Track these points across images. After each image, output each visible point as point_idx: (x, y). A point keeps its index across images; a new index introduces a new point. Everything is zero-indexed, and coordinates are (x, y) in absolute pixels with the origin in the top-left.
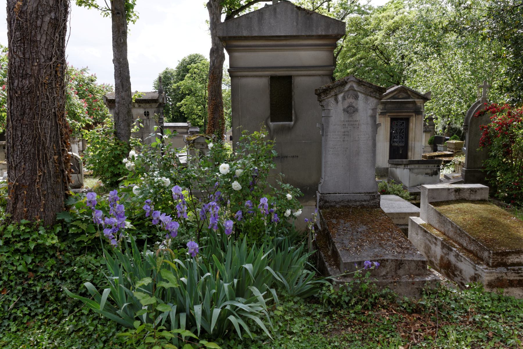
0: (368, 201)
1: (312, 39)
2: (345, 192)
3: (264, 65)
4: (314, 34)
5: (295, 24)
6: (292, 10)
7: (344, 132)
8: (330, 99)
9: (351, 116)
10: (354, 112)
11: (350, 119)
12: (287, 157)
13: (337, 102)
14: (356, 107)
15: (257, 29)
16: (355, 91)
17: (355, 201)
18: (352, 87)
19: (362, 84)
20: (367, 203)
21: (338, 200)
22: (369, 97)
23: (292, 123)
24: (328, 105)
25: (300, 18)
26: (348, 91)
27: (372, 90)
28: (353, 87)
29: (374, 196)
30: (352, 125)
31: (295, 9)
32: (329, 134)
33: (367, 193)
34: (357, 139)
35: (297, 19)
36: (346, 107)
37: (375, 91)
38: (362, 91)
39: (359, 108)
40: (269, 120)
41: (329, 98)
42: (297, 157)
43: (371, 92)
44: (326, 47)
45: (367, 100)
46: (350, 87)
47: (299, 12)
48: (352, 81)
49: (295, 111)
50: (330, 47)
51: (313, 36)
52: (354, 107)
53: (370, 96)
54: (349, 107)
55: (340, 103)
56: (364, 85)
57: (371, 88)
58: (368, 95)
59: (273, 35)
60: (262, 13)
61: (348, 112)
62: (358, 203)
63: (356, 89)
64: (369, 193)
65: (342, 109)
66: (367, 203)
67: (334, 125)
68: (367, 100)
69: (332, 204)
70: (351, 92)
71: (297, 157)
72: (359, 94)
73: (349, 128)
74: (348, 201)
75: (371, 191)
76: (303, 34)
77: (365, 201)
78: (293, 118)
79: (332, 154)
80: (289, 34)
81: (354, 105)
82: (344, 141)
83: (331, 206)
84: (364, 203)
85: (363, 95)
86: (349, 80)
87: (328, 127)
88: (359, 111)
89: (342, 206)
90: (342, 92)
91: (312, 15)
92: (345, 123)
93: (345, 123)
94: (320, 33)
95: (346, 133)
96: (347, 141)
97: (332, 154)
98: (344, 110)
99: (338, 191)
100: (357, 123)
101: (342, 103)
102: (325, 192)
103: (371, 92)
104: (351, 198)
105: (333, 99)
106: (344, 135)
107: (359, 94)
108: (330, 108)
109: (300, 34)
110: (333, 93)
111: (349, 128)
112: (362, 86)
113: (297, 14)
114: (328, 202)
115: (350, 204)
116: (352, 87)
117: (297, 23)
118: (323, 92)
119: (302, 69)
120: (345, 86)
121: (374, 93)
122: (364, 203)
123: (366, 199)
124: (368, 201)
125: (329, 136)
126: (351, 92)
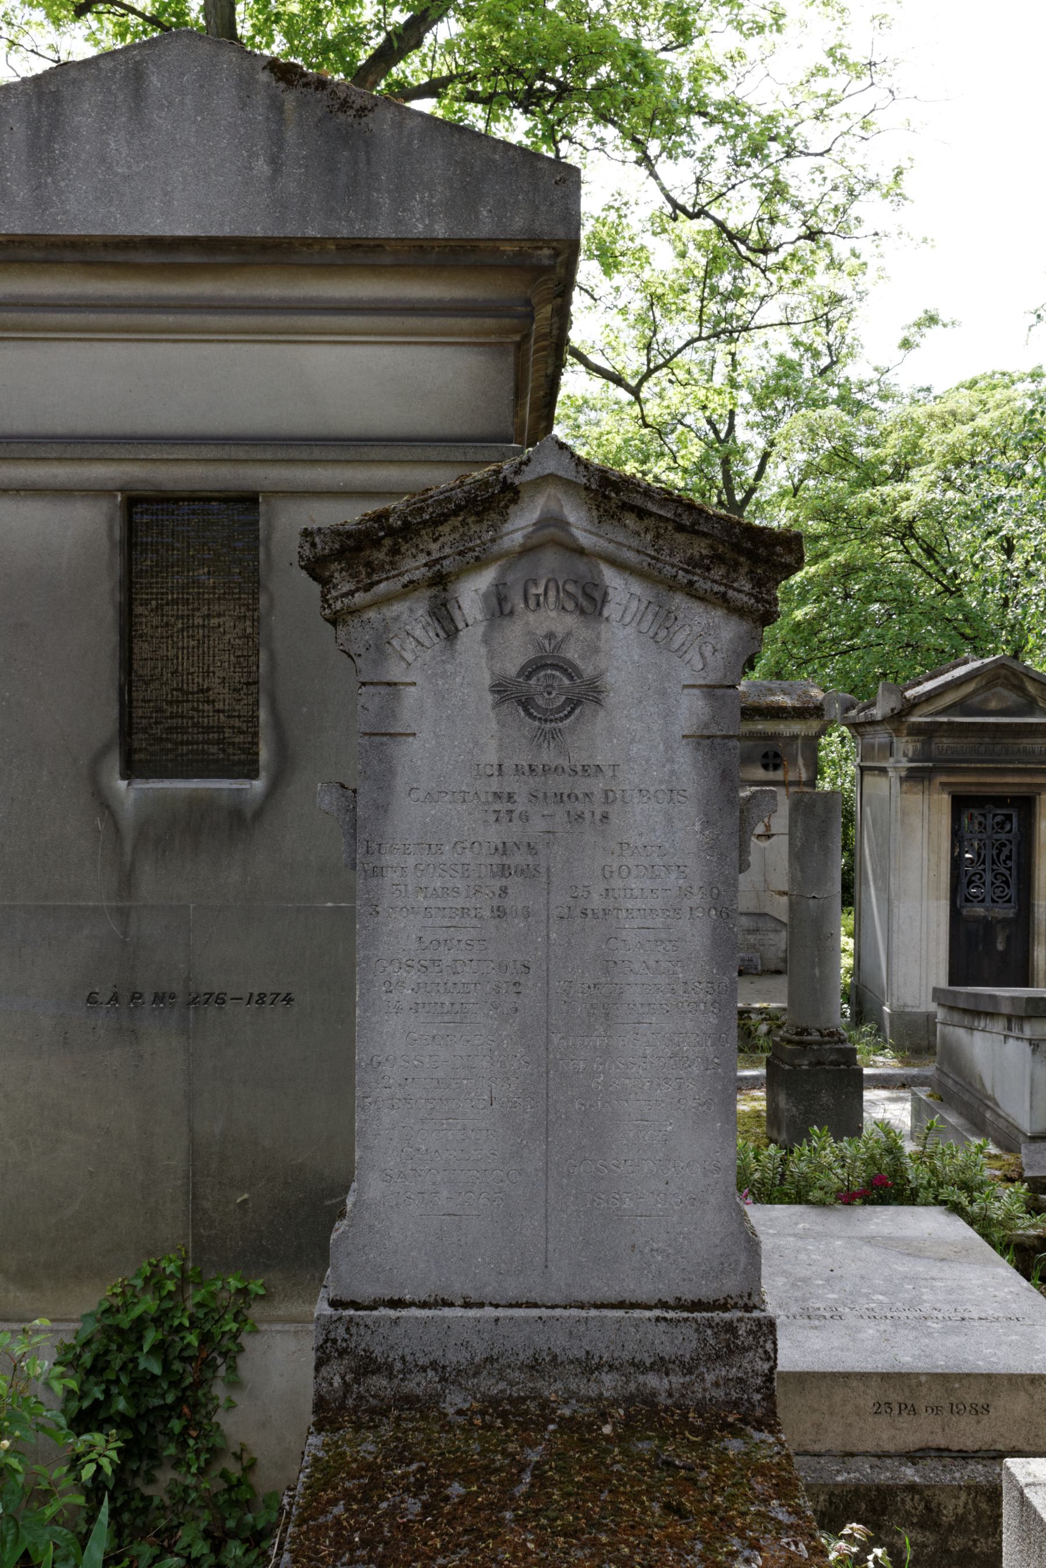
0: (688, 1369)
1: (375, 269)
2: (513, 1290)
3: (82, 425)
4: (383, 230)
5: (262, 167)
6: (245, 84)
7: (504, 849)
8: (397, 608)
9: (554, 734)
10: (573, 703)
11: (548, 756)
12: (220, 999)
13: (451, 634)
14: (588, 669)
15: (21, 193)
16: (580, 551)
17: (590, 1367)
18: (552, 521)
19: (627, 507)
20: (677, 1380)
21: (454, 1357)
22: (679, 600)
23: (258, 786)
24: (380, 648)
25: (291, 135)
26: (527, 550)
27: (700, 548)
28: (562, 524)
29: (730, 1328)
30: (560, 797)
31: (264, 77)
32: (388, 859)
33: (679, 1305)
34: (596, 901)
35: (278, 141)
36: (512, 669)
37: (718, 559)
38: (631, 557)
39: (611, 678)
40: (114, 763)
41: (389, 599)
42: (288, 999)
43: (693, 564)
44: (465, 323)
45: (666, 618)
46: (542, 523)
47: (290, 99)
48: (551, 478)
49: (274, 712)
50: (489, 322)
51: (377, 246)
52: (568, 669)
53: (690, 591)
54: (531, 669)
55: (470, 639)
56: (642, 513)
57: (692, 531)
58: (672, 586)
59: (124, 228)
60: (57, 98)
61: (526, 704)
62: (609, 1384)
63: (584, 539)
64: (697, 1306)
65: (487, 680)
66: (677, 1380)
67: (430, 797)
68: (666, 618)
69: (417, 1384)
70: (550, 560)
71: (288, 999)
72: (610, 577)
73: (538, 824)
74: (534, 1367)
75: (707, 1291)
76: (311, 233)
77: (661, 1365)
78: (264, 754)
79: (415, 1008)
80: (226, 231)
81: (572, 653)
82: (500, 913)
83: (408, 1401)
84: (652, 1381)
85: (637, 587)
86: (529, 474)
87: (383, 809)
88: (611, 699)
89: (492, 1403)
90: (480, 563)
91: (369, 119)
92: (512, 784)
93: (512, 784)
94: (419, 229)
95: (518, 859)
96: (527, 914)
97: (415, 1008)
98: (501, 690)
99: (459, 1288)
100: (598, 785)
101: (486, 640)
102: (367, 1291)
103: (693, 564)
104: (560, 1342)
105: (421, 610)
106: (504, 870)
107: (610, 577)
108: (395, 672)
109: (291, 230)
110: (414, 567)
111: (538, 824)
112: (630, 520)
113: (276, 106)
114: (386, 1369)
115: (551, 1391)
116: (552, 521)
117: (274, 161)
118: (338, 555)
119: (317, 453)
120: (504, 517)
121: (717, 573)
122: (652, 1381)
123: (668, 1350)
124: (688, 1369)
125: (391, 877)
126: (550, 560)
